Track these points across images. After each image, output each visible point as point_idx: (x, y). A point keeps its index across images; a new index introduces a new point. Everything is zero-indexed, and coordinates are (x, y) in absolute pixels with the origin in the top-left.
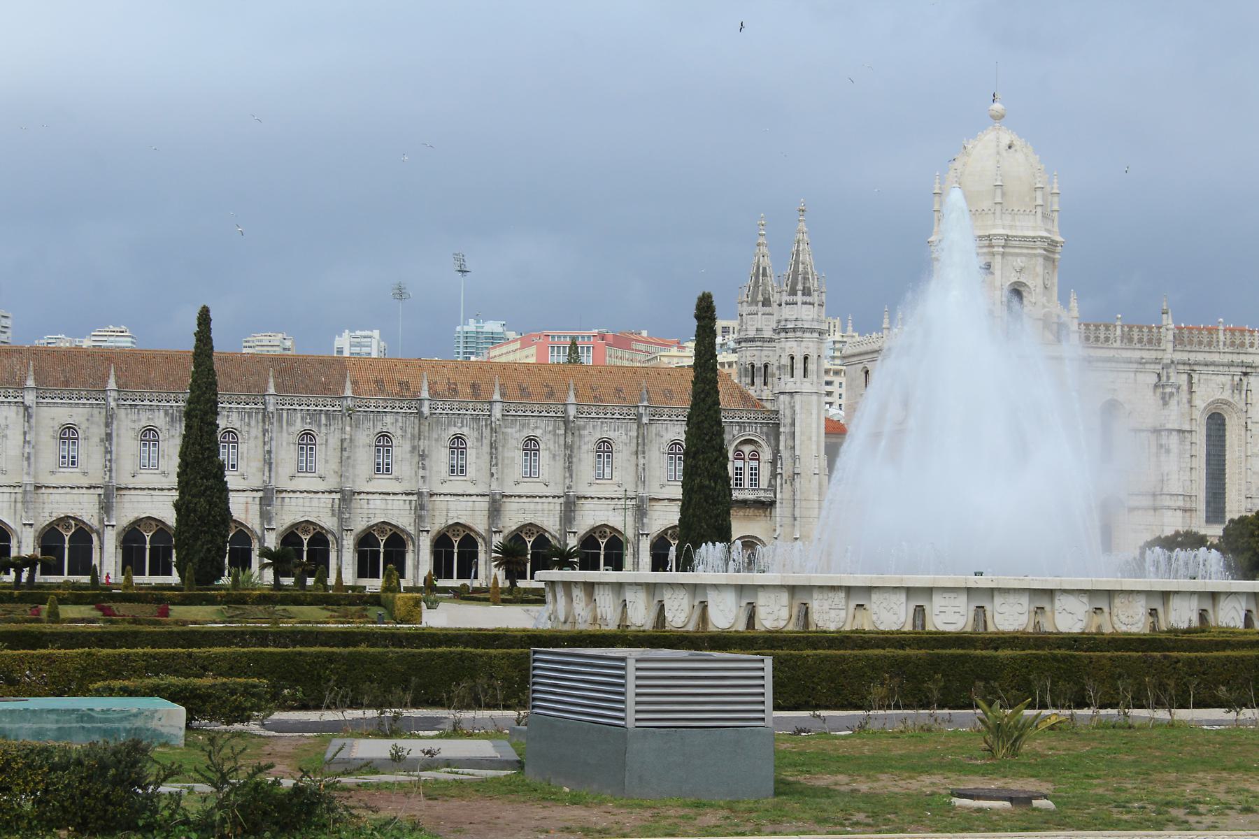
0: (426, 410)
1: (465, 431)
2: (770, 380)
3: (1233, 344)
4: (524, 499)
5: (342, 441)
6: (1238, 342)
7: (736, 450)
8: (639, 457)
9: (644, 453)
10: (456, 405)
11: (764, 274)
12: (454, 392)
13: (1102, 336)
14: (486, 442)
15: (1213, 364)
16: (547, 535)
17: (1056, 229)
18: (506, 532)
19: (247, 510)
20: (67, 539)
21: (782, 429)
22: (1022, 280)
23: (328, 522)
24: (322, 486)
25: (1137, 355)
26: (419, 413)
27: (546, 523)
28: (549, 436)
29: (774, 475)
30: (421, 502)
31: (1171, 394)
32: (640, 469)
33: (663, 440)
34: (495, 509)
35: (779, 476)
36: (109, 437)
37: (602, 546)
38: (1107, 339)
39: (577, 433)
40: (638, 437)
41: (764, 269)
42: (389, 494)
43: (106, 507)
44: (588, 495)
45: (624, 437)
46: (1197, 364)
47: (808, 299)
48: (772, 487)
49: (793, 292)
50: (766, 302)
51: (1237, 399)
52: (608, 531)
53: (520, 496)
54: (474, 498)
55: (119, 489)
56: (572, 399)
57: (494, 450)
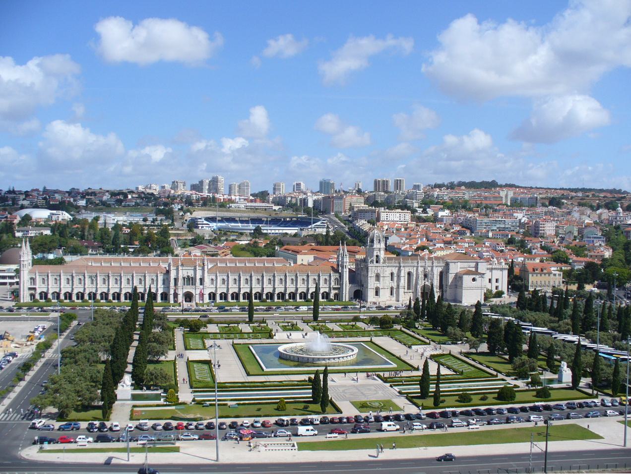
0: (287, 275)
12: (292, 272)
34: (297, 289)
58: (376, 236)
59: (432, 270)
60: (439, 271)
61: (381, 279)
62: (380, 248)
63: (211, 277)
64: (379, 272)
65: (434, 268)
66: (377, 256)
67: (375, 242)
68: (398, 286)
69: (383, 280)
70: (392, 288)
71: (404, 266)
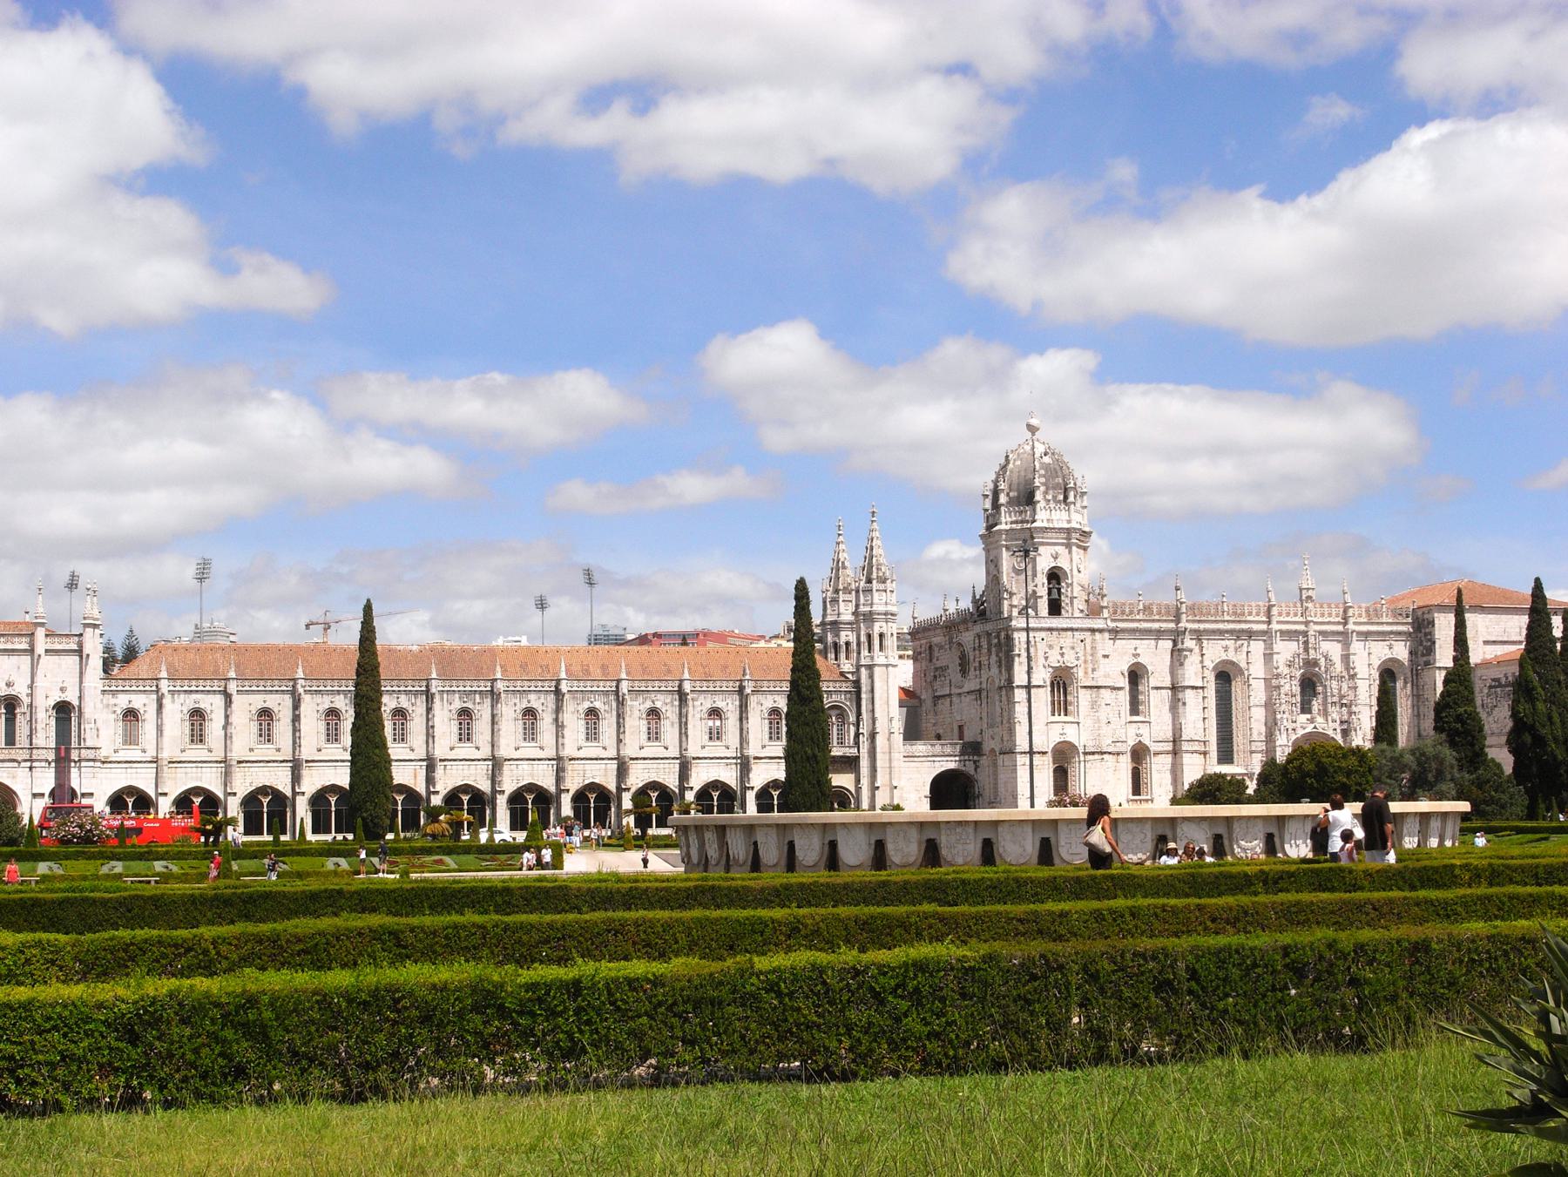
1: (597, 704)
3: (1235, 613)
5: (493, 716)
6: (1239, 611)
8: (744, 722)
10: (589, 683)
11: (844, 567)
12: (587, 672)
13: (1127, 610)
14: (614, 713)
15: (1221, 632)
17: (1085, 522)
18: (633, 790)
19: (415, 777)
20: (265, 804)
21: (864, 696)
22: (1059, 565)
23: (484, 786)
24: (478, 755)
25: (1156, 626)
26: (557, 692)
28: (668, 707)
30: (559, 765)
31: (1186, 656)
32: (744, 732)
33: (763, 708)
34: (622, 772)
36: (296, 719)
37: (715, 798)
38: (1131, 613)
39: (690, 703)
41: (843, 563)
42: (534, 760)
43: (296, 779)
44: (701, 756)
46: (1206, 631)
47: (882, 586)
48: (857, 743)
49: (869, 581)
50: (847, 590)
51: (1240, 659)
53: (645, 759)
55: (307, 761)
56: (686, 676)
58: (1046, 467)
59: (1346, 658)
60: (1376, 663)
61: (1084, 698)
62: (1069, 531)
63: (123, 701)
64: (1070, 660)
65: (1357, 646)
66: (1055, 576)
67: (1038, 496)
68: (1176, 740)
69: (1094, 705)
70: (1139, 754)
71: (1199, 635)
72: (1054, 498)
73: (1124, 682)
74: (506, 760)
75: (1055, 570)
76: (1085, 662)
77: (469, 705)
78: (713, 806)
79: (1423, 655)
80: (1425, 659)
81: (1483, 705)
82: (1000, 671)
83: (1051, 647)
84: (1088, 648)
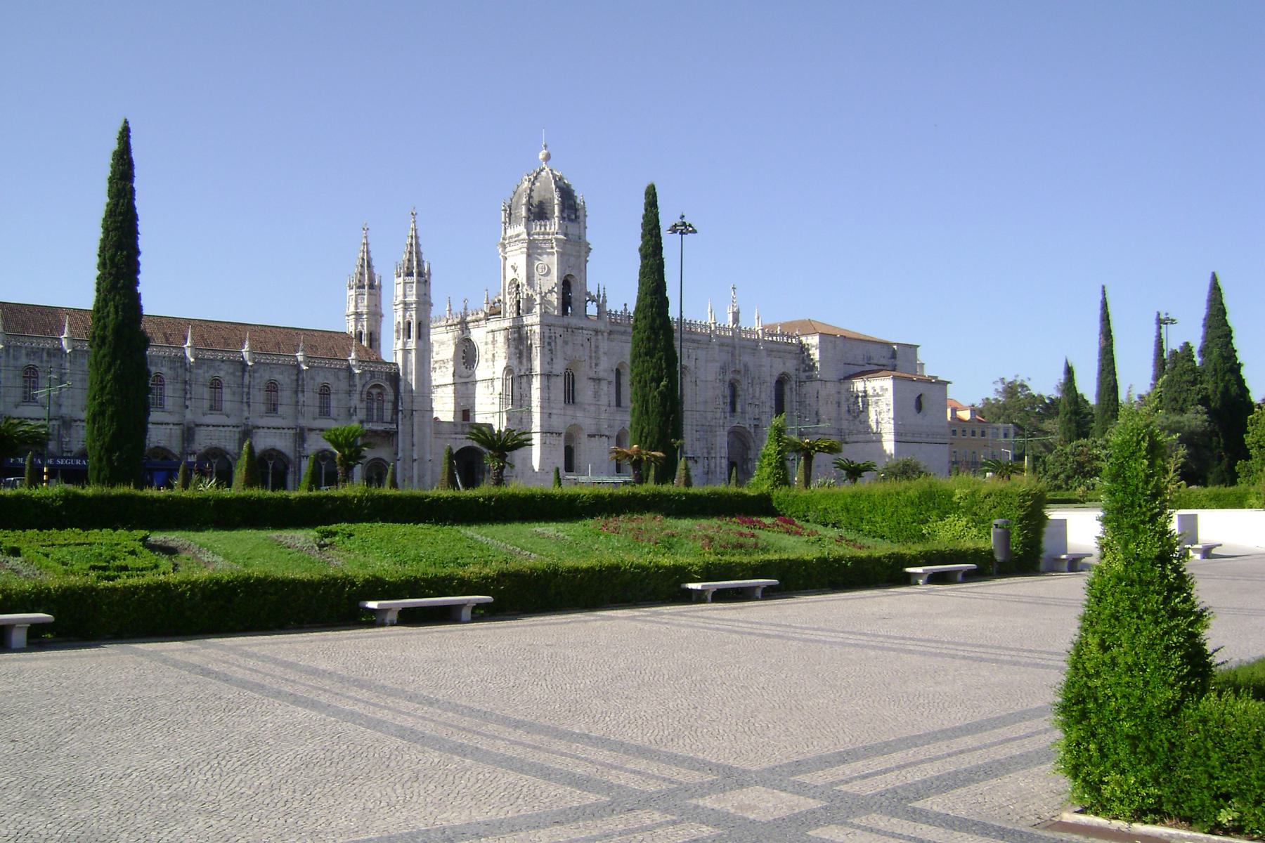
2: (374, 344)
4: (211, 428)
7: (369, 393)
8: (300, 395)
9: (303, 392)
16: (228, 456)
27: (228, 447)
29: (396, 410)
35: (400, 413)
37: (270, 466)
40: (297, 380)
45: (287, 379)
48: (394, 420)
52: (275, 454)
53: (208, 426)
54: (171, 426)
57: (188, 387)
69: (596, 395)
72: (568, 216)
73: (613, 377)
74: (75, 421)
75: (569, 279)
76: (591, 357)
77: (37, 363)
78: (268, 473)
79: (805, 371)
80: (807, 374)
81: (849, 411)
82: (521, 362)
83: (566, 343)
84: (593, 346)
